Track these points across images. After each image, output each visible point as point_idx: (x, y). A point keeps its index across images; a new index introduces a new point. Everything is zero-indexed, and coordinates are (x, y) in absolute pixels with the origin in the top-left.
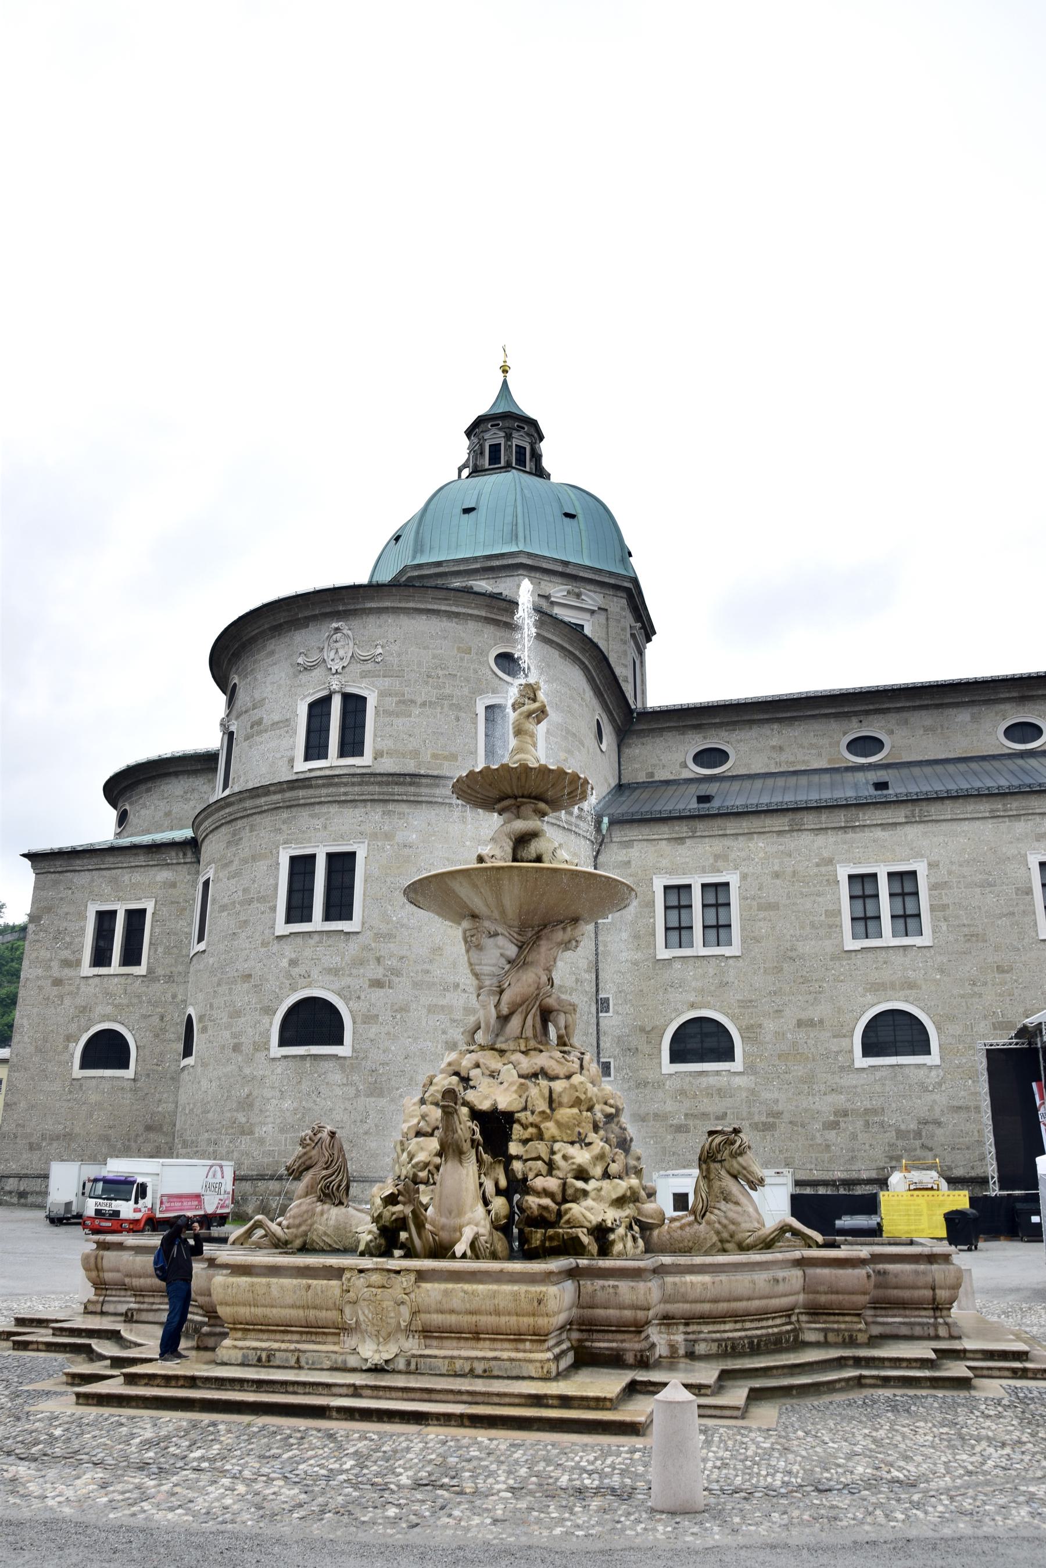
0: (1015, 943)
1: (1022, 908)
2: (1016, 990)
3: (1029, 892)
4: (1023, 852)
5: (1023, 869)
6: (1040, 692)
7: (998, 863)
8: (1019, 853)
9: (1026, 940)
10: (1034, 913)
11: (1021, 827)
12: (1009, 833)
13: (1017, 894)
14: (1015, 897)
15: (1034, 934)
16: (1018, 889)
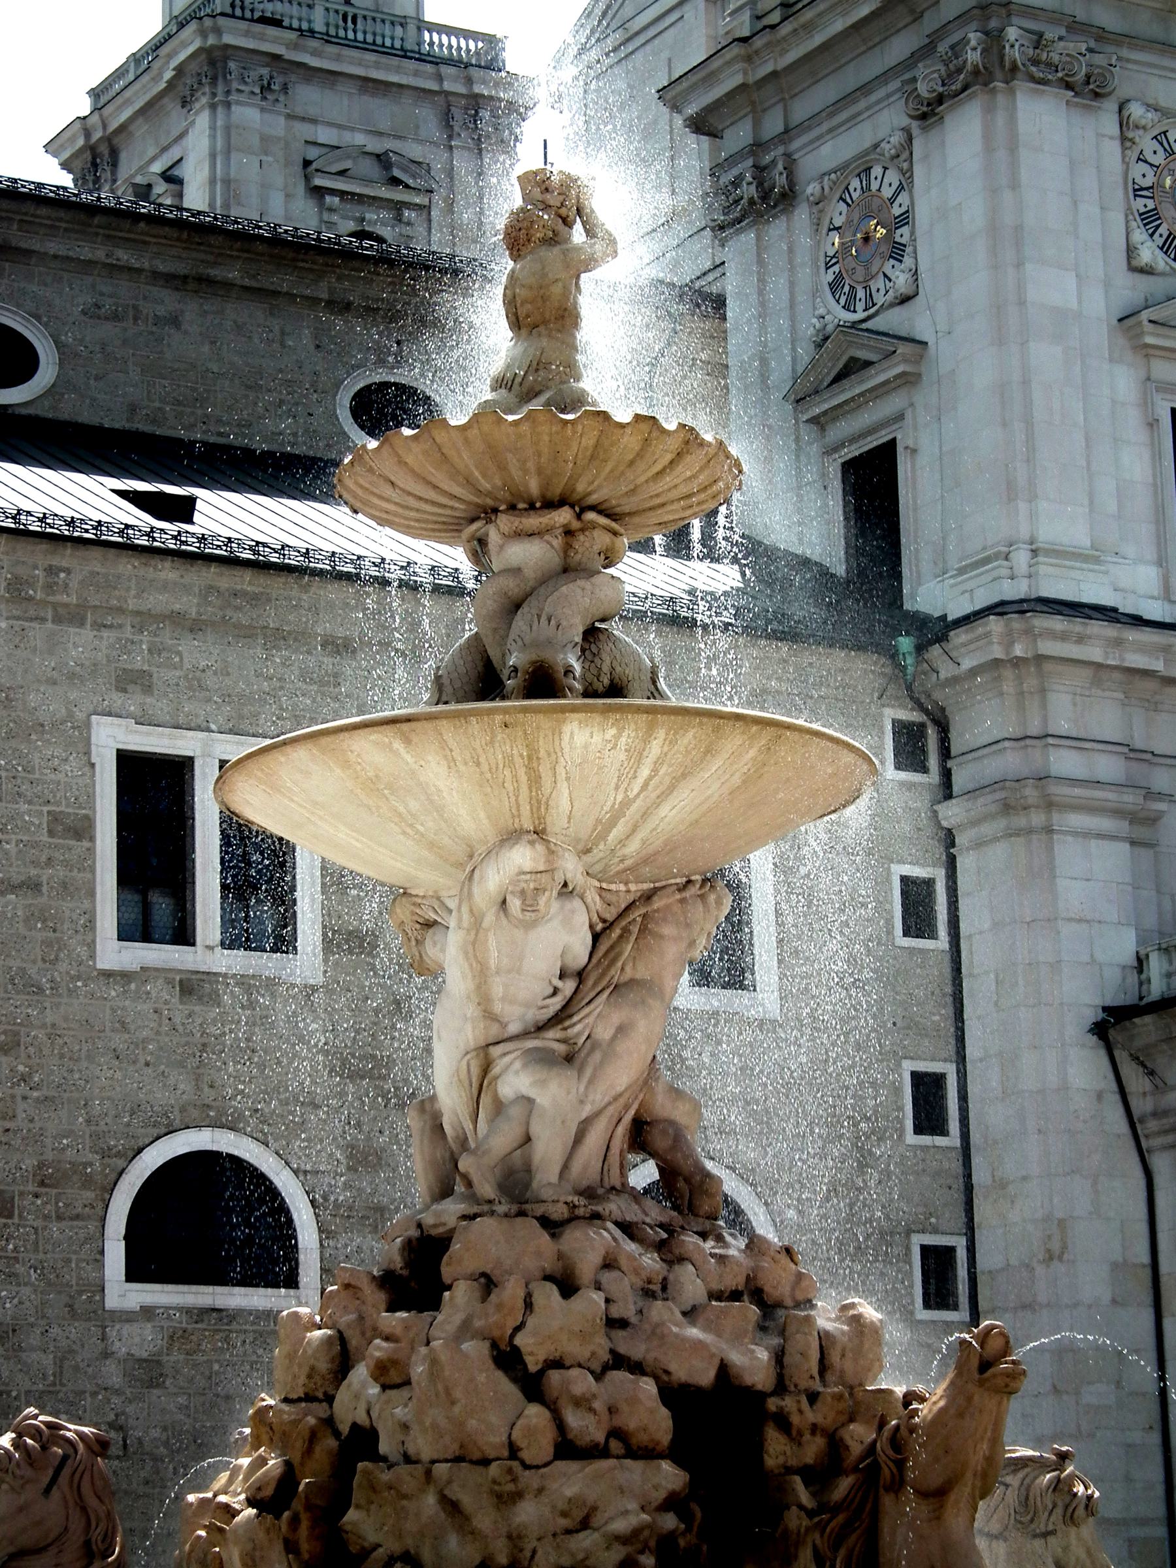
0: (32, 971)
1: (61, 872)
2: (21, 1106)
3: (83, 830)
4: (80, 715)
5: (73, 766)
6: (53, 247)
7: (10, 736)
8: (70, 715)
9: (63, 966)
10: (92, 894)
11: (81, 645)
12: (51, 652)
13: (51, 833)
14: (45, 838)
15: (82, 951)
16: (55, 818)
